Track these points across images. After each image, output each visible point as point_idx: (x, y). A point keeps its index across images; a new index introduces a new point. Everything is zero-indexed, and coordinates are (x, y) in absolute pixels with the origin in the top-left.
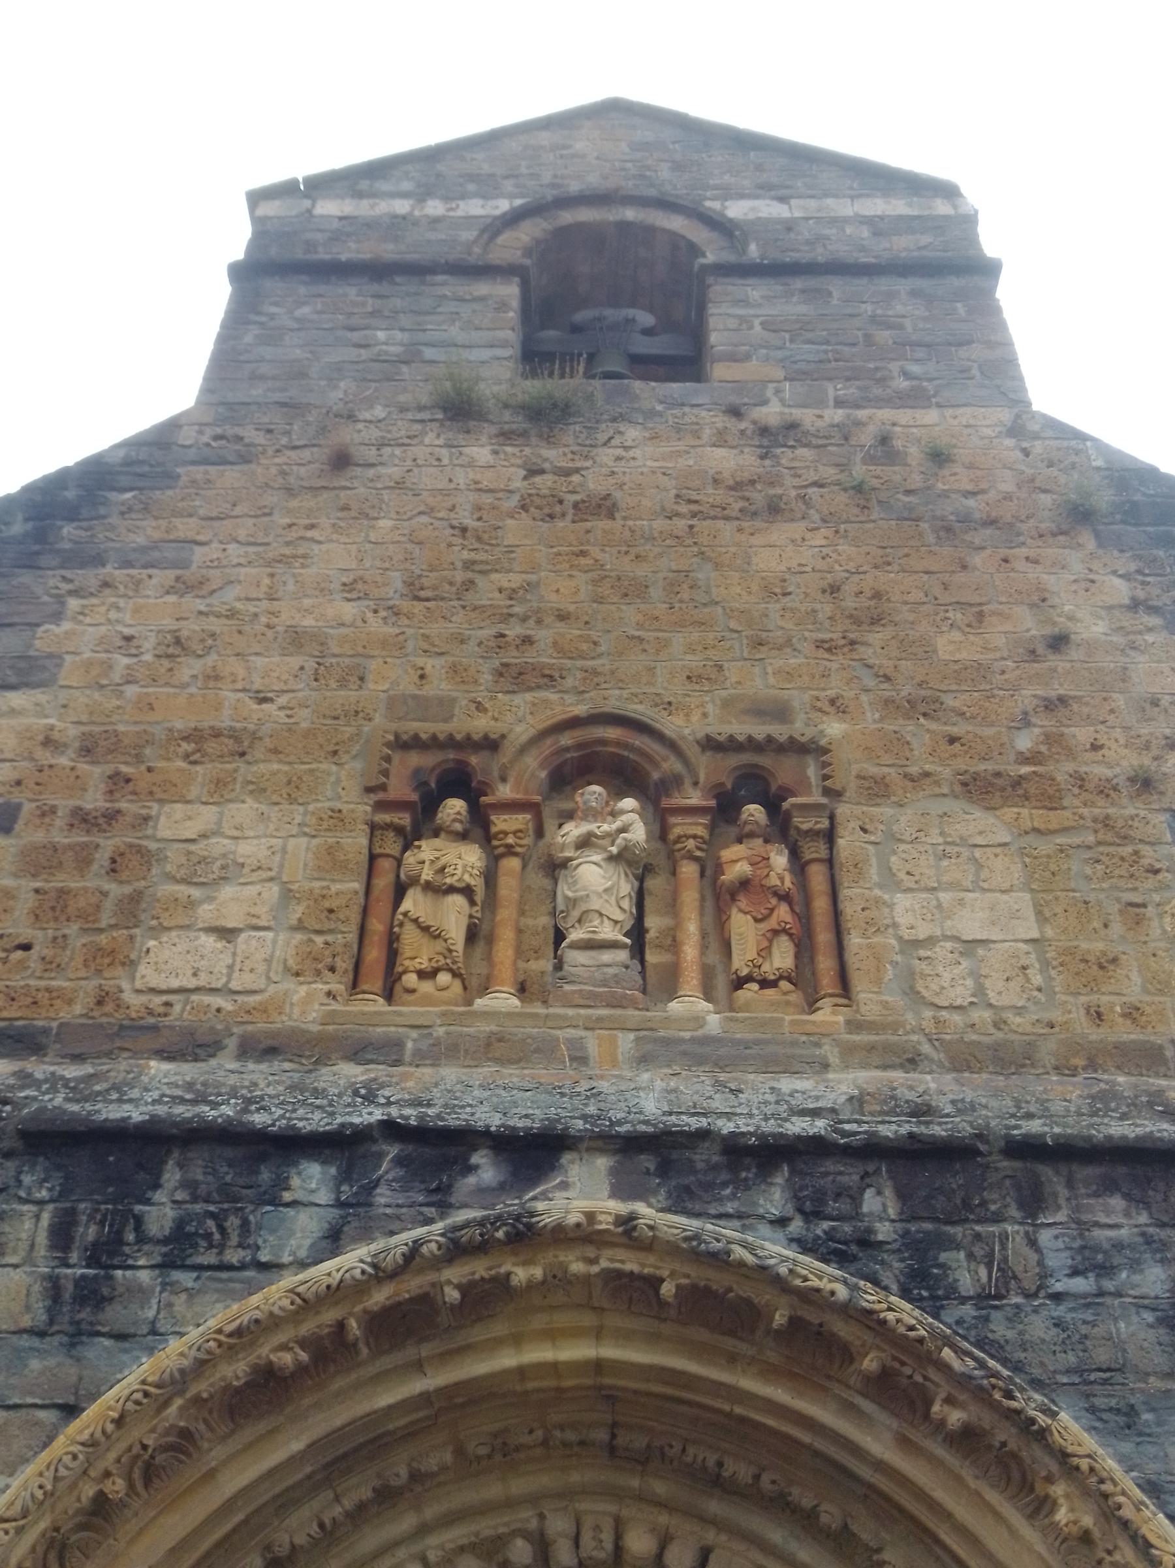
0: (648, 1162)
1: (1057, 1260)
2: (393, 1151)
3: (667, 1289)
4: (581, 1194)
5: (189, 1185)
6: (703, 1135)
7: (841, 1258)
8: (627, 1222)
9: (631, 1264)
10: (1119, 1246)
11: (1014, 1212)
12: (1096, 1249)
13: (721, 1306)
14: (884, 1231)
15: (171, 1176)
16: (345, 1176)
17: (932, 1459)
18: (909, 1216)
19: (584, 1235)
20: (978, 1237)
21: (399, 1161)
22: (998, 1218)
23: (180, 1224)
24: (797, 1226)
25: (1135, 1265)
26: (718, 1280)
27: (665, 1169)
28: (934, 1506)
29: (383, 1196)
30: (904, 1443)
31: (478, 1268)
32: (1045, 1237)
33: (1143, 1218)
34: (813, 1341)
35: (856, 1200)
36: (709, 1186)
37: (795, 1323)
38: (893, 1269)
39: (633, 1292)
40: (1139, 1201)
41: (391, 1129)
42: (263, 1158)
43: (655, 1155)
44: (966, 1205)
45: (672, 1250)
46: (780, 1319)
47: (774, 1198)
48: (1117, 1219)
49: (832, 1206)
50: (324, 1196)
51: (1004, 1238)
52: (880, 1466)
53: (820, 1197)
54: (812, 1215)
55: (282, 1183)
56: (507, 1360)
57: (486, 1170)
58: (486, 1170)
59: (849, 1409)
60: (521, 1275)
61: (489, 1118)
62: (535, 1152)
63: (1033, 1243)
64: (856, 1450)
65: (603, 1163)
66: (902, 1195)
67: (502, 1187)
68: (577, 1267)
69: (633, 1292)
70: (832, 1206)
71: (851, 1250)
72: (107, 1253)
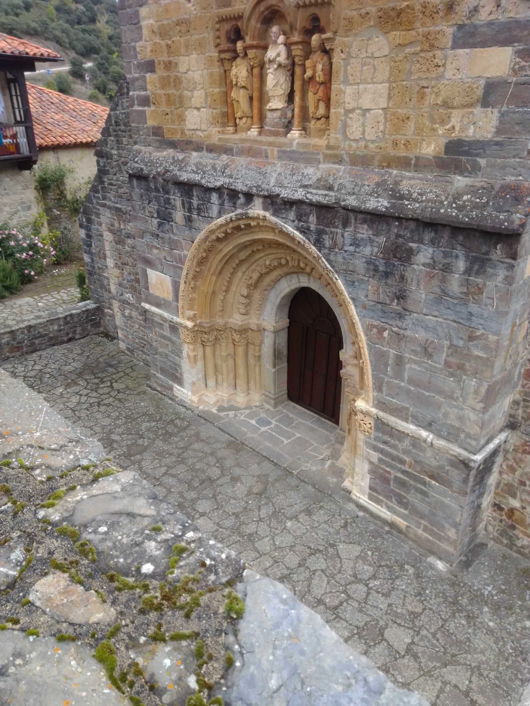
1: (348, 241)
10: (362, 239)
11: (340, 226)
12: (357, 240)
18: (318, 224)
20: (331, 232)
22: (337, 227)
25: (365, 246)
27: (273, 203)
32: (346, 234)
33: (370, 232)
36: (280, 209)
40: (370, 227)
44: (331, 223)
47: (292, 215)
51: (337, 233)
63: (343, 236)
66: (318, 218)
71: (304, 231)
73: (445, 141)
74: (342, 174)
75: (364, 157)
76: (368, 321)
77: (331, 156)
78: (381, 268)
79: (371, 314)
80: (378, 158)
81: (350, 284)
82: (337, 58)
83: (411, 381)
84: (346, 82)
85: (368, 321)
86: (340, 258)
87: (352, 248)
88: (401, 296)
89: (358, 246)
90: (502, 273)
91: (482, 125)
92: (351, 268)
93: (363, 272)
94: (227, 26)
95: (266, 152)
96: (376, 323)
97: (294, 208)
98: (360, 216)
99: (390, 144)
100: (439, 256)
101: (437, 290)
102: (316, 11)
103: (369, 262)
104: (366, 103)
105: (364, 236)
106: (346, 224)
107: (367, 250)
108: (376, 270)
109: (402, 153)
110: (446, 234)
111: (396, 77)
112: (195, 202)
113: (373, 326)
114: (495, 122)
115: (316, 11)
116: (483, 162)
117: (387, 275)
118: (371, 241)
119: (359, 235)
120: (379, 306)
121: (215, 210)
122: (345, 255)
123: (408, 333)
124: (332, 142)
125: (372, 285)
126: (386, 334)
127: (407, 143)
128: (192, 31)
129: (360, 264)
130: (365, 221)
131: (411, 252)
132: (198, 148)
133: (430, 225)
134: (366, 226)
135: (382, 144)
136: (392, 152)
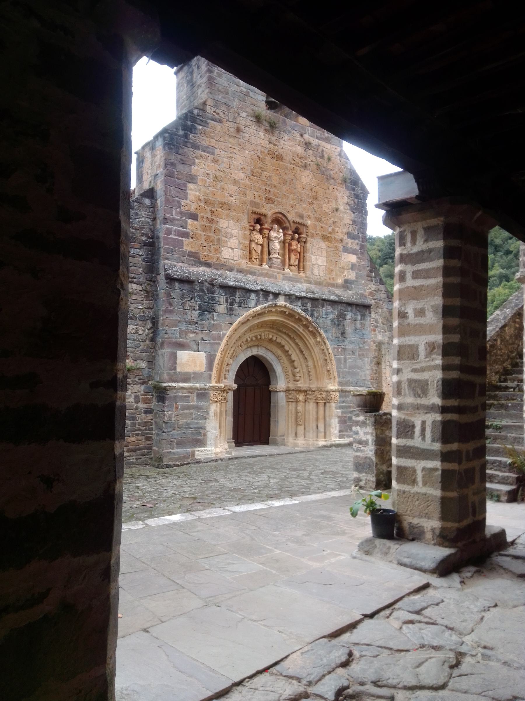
0: (288, 297)
1: (324, 313)
2: (262, 293)
3: (287, 313)
4: (281, 301)
5: (240, 295)
6: (294, 294)
7: (305, 311)
8: (286, 305)
9: (284, 310)
13: (291, 315)
14: (309, 309)
15: (237, 294)
16: (257, 296)
17: (306, 332)
19: (281, 307)
21: (262, 294)
23: (240, 301)
24: (301, 307)
26: (292, 312)
27: (289, 298)
28: (304, 336)
29: (261, 299)
30: (303, 330)
31: (269, 309)
34: (300, 320)
35: (307, 304)
37: (298, 318)
38: (309, 313)
39: (283, 313)
40: (332, 307)
41: (262, 290)
42: (247, 292)
43: (289, 297)
45: (289, 309)
46: (297, 317)
48: (330, 309)
49: (305, 305)
50: (255, 299)
52: (301, 333)
53: (304, 304)
54: (303, 306)
55: (250, 296)
56: (268, 319)
57: (271, 297)
58: (271, 297)
59: (299, 326)
60: (274, 310)
61: (273, 290)
62: (276, 295)
64: (299, 331)
65: (283, 297)
67: (273, 299)
68: (279, 310)
69: (283, 313)
70: (305, 305)
72: (232, 304)
73: (344, 279)
74: (313, 287)
75: (320, 282)
76: (333, 346)
77: (307, 280)
78: (336, 323)
79: (334, 343)
80: (324, 282)
81: (326, 331)
82: (308, 245)
83: (350, 367)
84: (312, 254)
85: (333, 346)
86: (321, 321)
87: (325, 316)
88: (343, 333)
89: (328, 315)
90: (369, 318)
91: (352, 275)
92: (326, 324)
93: (330, 325)
94: (256, 217)
95: (276, 276)
96: (336, 346)
97: (300, 301)
98: (328, 303)
99: (328, 279)
100: (353, 315)
101: (354, 328)
102: (299, 226)
103: (332, 321)
104: (319, 262)
105: (330, 311)
106: (323, 306)
107: (331, 316)
108: (335, 324)
109: (332, 282)
110: (354, 307)
111: (328, 256)
112: (237, 299)
113: (335, 348)
114: (355, 275)
115: (299, 226)
116: (353, 286)
117: (338, 325)
118: (332, 312)
119: (328, 311)
120: (337, 339)
121: (252, 303)
122: (323, 319)
123: (347, 347)
124: (308, 275)
125: (334, 330)
126: (340, 350)
127: (333, 279)
128: (232, 210)
129: (329, 322)
130: (329, 305)
131: (345, 315)
132: (231, 270)
133: (349, 304)
134: (330, 307)
135: (325, 278)
136: (329, 281)
